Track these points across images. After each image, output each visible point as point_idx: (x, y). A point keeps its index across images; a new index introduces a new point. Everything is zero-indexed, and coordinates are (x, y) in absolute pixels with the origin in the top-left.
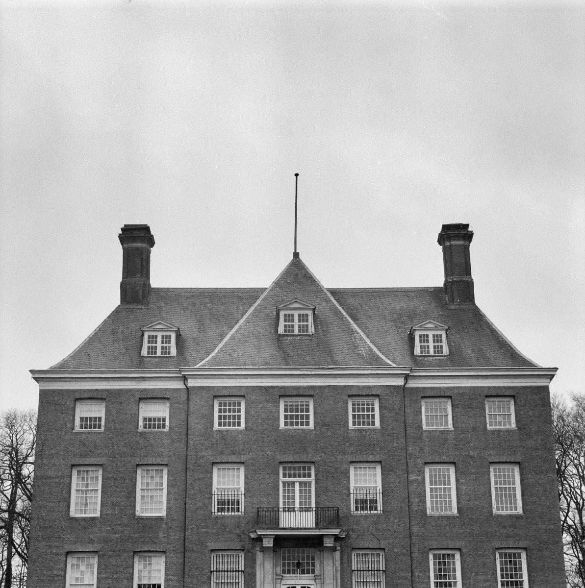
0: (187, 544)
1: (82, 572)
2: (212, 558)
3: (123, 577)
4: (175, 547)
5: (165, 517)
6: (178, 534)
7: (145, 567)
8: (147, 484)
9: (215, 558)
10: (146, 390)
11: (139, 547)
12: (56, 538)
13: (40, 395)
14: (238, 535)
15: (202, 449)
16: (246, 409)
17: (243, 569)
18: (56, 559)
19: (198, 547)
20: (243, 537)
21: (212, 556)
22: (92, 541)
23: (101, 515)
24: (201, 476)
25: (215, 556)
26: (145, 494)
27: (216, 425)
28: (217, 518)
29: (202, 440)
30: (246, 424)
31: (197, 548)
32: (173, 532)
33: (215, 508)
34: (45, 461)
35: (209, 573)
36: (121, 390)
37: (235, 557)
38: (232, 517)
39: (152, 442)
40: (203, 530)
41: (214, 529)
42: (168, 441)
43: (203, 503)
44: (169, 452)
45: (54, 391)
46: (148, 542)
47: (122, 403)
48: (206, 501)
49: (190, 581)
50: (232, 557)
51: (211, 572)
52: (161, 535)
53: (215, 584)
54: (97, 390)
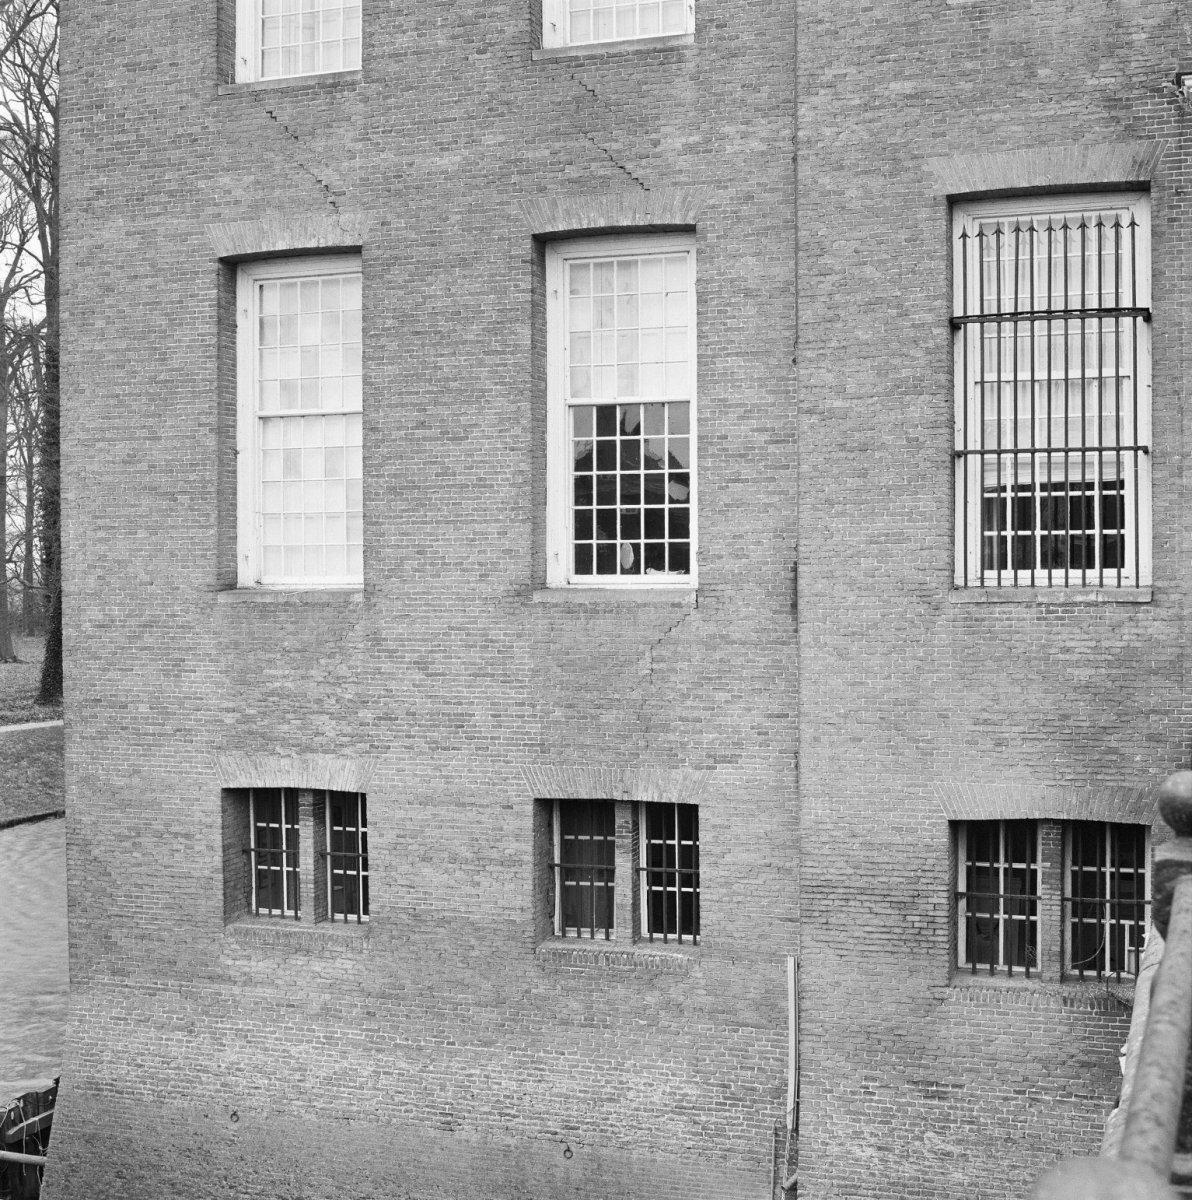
0: (805, 171)
1: (309, 353)
2: (958, 244)
3: (484, 372)
4: (749, 197)
5: (691, 40)
6: (763, 127)
9: (973, 243)
12: (171, 194)
14: (1112, 102)
17: (1143, 302)
18: (175, 297)
19: (876, 183)
20: (1144, 109)
21: (957, 232)
22: (331, 198)
23: (367, 60)
25: (973, 230)
31: (868, 194)
32: (731, 121)
35: (942, 332)
37: (1092, 232)
40: (896, 86)
41: (964, 74)
49: (830, 378)
51: (955, 325)
52: (674, 140)
53: (974, 393)
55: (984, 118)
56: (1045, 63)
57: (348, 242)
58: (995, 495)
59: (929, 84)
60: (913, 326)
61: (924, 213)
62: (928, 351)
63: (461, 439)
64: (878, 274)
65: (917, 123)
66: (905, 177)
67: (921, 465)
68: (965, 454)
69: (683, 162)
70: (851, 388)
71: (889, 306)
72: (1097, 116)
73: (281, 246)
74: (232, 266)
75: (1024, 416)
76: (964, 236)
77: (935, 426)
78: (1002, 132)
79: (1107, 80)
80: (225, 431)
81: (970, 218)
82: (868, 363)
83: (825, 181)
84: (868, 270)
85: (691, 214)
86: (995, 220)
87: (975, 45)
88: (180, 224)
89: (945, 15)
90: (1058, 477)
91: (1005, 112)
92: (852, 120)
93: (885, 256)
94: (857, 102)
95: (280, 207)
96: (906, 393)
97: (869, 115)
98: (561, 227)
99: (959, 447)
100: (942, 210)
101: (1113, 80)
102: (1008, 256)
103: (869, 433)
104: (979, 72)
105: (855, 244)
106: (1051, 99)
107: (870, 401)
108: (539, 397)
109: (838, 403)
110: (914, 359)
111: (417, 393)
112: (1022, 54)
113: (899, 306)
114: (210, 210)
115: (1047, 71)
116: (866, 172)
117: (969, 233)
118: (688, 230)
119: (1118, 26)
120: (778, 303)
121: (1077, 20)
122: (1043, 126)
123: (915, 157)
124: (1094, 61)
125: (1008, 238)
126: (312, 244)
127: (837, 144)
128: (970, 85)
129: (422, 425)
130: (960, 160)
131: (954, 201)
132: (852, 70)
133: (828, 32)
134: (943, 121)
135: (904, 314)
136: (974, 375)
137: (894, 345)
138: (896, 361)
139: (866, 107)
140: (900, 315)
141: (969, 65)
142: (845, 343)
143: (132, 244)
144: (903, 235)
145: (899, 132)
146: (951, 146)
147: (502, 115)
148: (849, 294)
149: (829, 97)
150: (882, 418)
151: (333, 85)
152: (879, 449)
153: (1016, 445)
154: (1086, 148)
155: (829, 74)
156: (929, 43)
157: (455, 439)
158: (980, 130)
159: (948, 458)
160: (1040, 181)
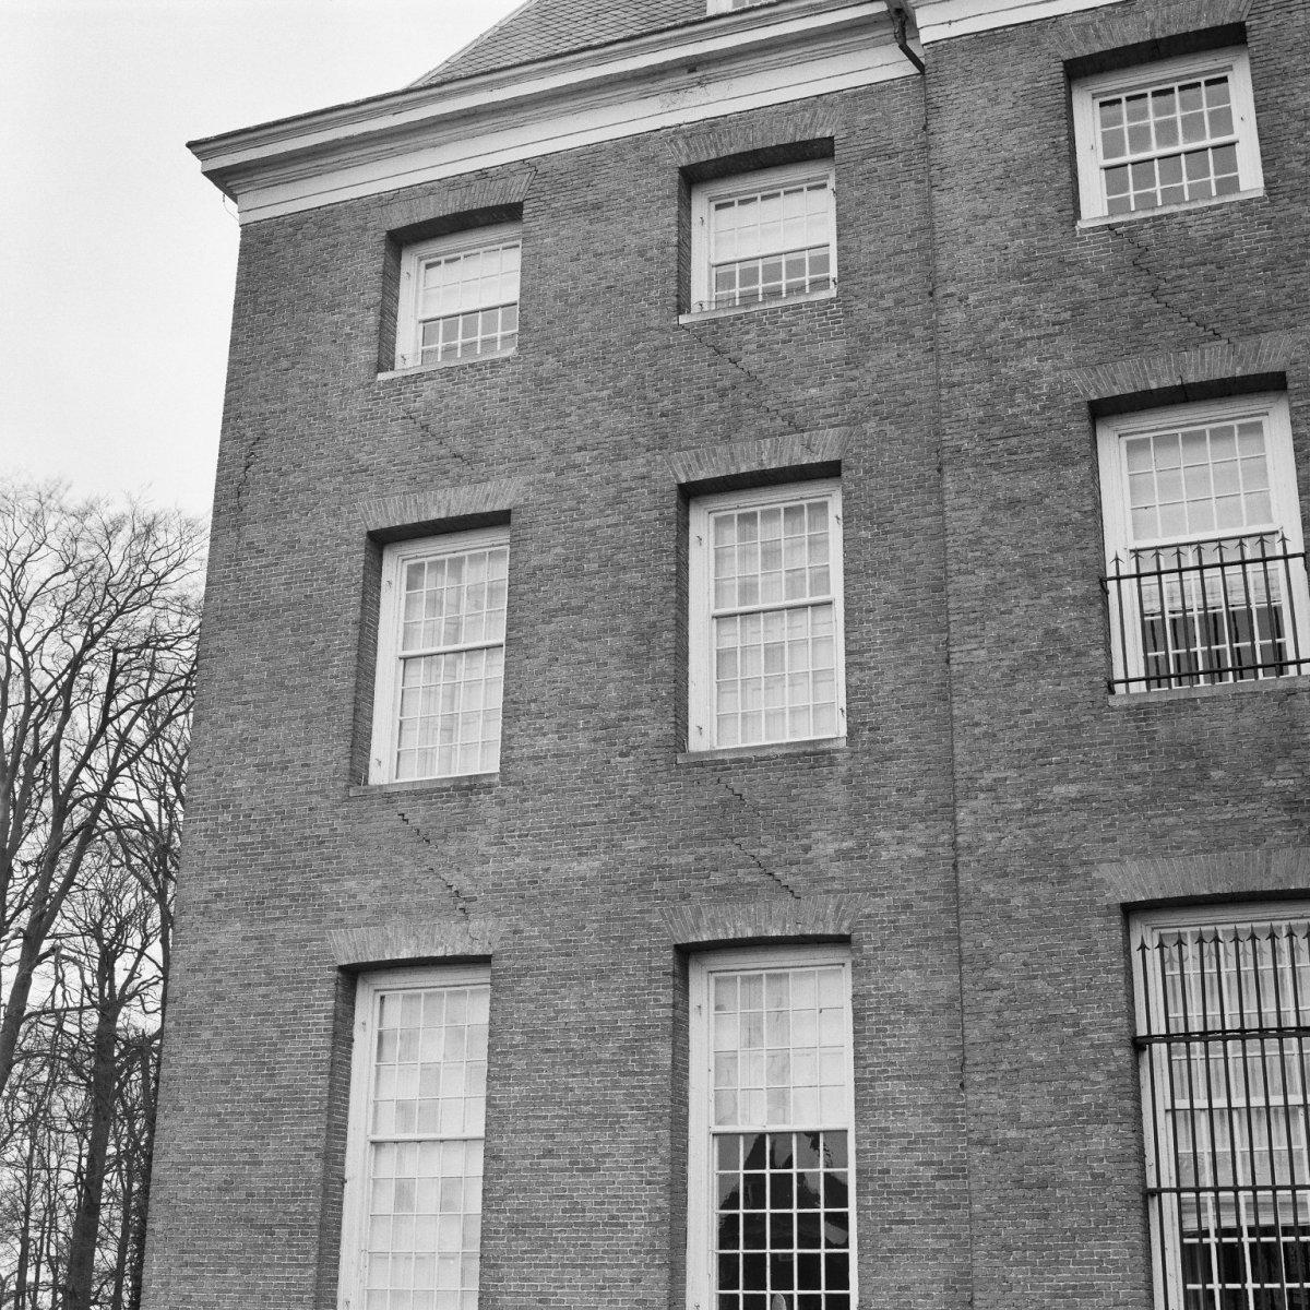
0: (966, 878)
1: (430, 1072)
2: (1136, 956)
3: (619, 1094)
4: (907, 906)
5: (843, 744)
6: (919, 831)
7: (753, 1028)
8: (747, 590)
9: (1153, 956)
10: (713, 125)
11: (704, 922)
12: (293, 898)
13: (245, 249)
15: (1020, 344)
16: (1256, 87)
18: (289, 1007)
19: (1042, 891)
21: (1136, 945)
22: (461, 905)
23: (505, 761)
24: (1026, 485)
25: (1152, 942)
26: (733, 636)
27: (1095, 205)
28: (1140, 712)
29: (1015, 292)
30: (1267, 163)
31: (1034, 902)
32: (887, 825)
33: (1130, 658)
34: (256, 533)
35: (1123, 1054)
36: (595, 149)
37: (1284, 943)
38: (1239, 701)
39: (752, 361)
41: (1132, 777)
42: (838, 348)
43: (1051, 634)
44: (849, 394)
45: (298, 222)
46: (752, 891)
47: (597, 206)
48: (1065, 622)
49: (1002, 1105)
50: (1265, 945)
51: (1139, 1045)
52: (826, 846)
53: (1165, 1122)
54: (483, 174)
55: (1156, 821)
56: (1218, 765)
57: (478, 950)
58: (1196, 1240)
59: (1095, 787)
60: (1092, 1046)
61: (1097, 923)
62: (1110, 1075)
63: (594, 1170)
64: (1051, 989)
65: (1085, 827)
66: (1075, 884)
67: (1109, 1204)
68: (1158, 1192)
69: (835, 869)
70: (1026, 1116)
71: (1065, 1025)
72: (1277, 819)
73: (405, 954)
74: (352, 975)
75: (1223, 1148)
76: (1143, 947)
77: (1122, 1159)
78: (1177, 836)
79: (1286, 782)
80: (333, 1157)
81: (1149, 929)
82: (1044, 1088)
83: (988, 888)
84: (1039, 985)
85: (846, 924)
86: (1176, 930)
87: (1142, 747)
88: (299, 929)
89: (1108, 717)
90: (1266, 1220)
91: (1178, 815)
92: (1013, 825)
93: (1057, 970)
94: (1020, 806)
95: (407, 913)
96: (1086, 1122)
97: (1033, 820)
98: (705, 937)
99: (1152, 1184)
100: (1116, 921)
101: (1292, 782)
102: (1192, 970)
103: (1049, 1168)
104: (1147, 774)
105: (1024, 957)
106: (1227, 802)
107: (1047, 1131)
108: (679, 1125)
109: (1012, 1134)
110: (1095, 1083)
111: (545, 1117)
112: (1192, 756)
113: (1076, 1024)
114: (332, 915)
115: (1221, 773)
116: (1032, 880)
117: (1148, 944)
118: (841, 941)
119: (1293, 726)
120: (943, 1020)
121: (1248, 720)
122: (1221, 830)
123: (1085, 863)
124: (1270, 762)
125: (1191, 950)
126: (439, 953)
127: (1000, 850)
128: (1138, 789)
129: (549, 1153)
130: (1133, 867)
131: (1130, 911)
132: (1012, 773)
133: (985, 734)
134: (1112, 825)
135: (1079, 1034)
136: (1163, 1103)
137: (1072, 1068)
138: (1075, 1086)
139: (1029, 811)
140: (1076, 1034)
141: (1136, 768)
142: (1016, 1066)
143: (249, 950)
144: (1075, 947)
145: (1066, 837)
146: (1123, 852)
147: (645, 819)
148: (1019, 1011)
149: (989, 802)
150: (1063, 1150)
151: (469, 787)
152: (1060, 1186)
153: (1216, 1182)
154: (1269, 853)
155: (987, 778)
156: (1094, 745)
157: (586, 1170)
158: (1153, 835)
159: (1138, 1197)
160: (1220, 888)
